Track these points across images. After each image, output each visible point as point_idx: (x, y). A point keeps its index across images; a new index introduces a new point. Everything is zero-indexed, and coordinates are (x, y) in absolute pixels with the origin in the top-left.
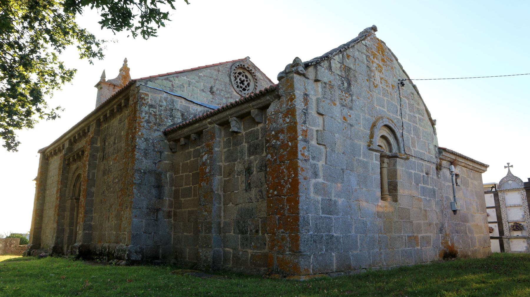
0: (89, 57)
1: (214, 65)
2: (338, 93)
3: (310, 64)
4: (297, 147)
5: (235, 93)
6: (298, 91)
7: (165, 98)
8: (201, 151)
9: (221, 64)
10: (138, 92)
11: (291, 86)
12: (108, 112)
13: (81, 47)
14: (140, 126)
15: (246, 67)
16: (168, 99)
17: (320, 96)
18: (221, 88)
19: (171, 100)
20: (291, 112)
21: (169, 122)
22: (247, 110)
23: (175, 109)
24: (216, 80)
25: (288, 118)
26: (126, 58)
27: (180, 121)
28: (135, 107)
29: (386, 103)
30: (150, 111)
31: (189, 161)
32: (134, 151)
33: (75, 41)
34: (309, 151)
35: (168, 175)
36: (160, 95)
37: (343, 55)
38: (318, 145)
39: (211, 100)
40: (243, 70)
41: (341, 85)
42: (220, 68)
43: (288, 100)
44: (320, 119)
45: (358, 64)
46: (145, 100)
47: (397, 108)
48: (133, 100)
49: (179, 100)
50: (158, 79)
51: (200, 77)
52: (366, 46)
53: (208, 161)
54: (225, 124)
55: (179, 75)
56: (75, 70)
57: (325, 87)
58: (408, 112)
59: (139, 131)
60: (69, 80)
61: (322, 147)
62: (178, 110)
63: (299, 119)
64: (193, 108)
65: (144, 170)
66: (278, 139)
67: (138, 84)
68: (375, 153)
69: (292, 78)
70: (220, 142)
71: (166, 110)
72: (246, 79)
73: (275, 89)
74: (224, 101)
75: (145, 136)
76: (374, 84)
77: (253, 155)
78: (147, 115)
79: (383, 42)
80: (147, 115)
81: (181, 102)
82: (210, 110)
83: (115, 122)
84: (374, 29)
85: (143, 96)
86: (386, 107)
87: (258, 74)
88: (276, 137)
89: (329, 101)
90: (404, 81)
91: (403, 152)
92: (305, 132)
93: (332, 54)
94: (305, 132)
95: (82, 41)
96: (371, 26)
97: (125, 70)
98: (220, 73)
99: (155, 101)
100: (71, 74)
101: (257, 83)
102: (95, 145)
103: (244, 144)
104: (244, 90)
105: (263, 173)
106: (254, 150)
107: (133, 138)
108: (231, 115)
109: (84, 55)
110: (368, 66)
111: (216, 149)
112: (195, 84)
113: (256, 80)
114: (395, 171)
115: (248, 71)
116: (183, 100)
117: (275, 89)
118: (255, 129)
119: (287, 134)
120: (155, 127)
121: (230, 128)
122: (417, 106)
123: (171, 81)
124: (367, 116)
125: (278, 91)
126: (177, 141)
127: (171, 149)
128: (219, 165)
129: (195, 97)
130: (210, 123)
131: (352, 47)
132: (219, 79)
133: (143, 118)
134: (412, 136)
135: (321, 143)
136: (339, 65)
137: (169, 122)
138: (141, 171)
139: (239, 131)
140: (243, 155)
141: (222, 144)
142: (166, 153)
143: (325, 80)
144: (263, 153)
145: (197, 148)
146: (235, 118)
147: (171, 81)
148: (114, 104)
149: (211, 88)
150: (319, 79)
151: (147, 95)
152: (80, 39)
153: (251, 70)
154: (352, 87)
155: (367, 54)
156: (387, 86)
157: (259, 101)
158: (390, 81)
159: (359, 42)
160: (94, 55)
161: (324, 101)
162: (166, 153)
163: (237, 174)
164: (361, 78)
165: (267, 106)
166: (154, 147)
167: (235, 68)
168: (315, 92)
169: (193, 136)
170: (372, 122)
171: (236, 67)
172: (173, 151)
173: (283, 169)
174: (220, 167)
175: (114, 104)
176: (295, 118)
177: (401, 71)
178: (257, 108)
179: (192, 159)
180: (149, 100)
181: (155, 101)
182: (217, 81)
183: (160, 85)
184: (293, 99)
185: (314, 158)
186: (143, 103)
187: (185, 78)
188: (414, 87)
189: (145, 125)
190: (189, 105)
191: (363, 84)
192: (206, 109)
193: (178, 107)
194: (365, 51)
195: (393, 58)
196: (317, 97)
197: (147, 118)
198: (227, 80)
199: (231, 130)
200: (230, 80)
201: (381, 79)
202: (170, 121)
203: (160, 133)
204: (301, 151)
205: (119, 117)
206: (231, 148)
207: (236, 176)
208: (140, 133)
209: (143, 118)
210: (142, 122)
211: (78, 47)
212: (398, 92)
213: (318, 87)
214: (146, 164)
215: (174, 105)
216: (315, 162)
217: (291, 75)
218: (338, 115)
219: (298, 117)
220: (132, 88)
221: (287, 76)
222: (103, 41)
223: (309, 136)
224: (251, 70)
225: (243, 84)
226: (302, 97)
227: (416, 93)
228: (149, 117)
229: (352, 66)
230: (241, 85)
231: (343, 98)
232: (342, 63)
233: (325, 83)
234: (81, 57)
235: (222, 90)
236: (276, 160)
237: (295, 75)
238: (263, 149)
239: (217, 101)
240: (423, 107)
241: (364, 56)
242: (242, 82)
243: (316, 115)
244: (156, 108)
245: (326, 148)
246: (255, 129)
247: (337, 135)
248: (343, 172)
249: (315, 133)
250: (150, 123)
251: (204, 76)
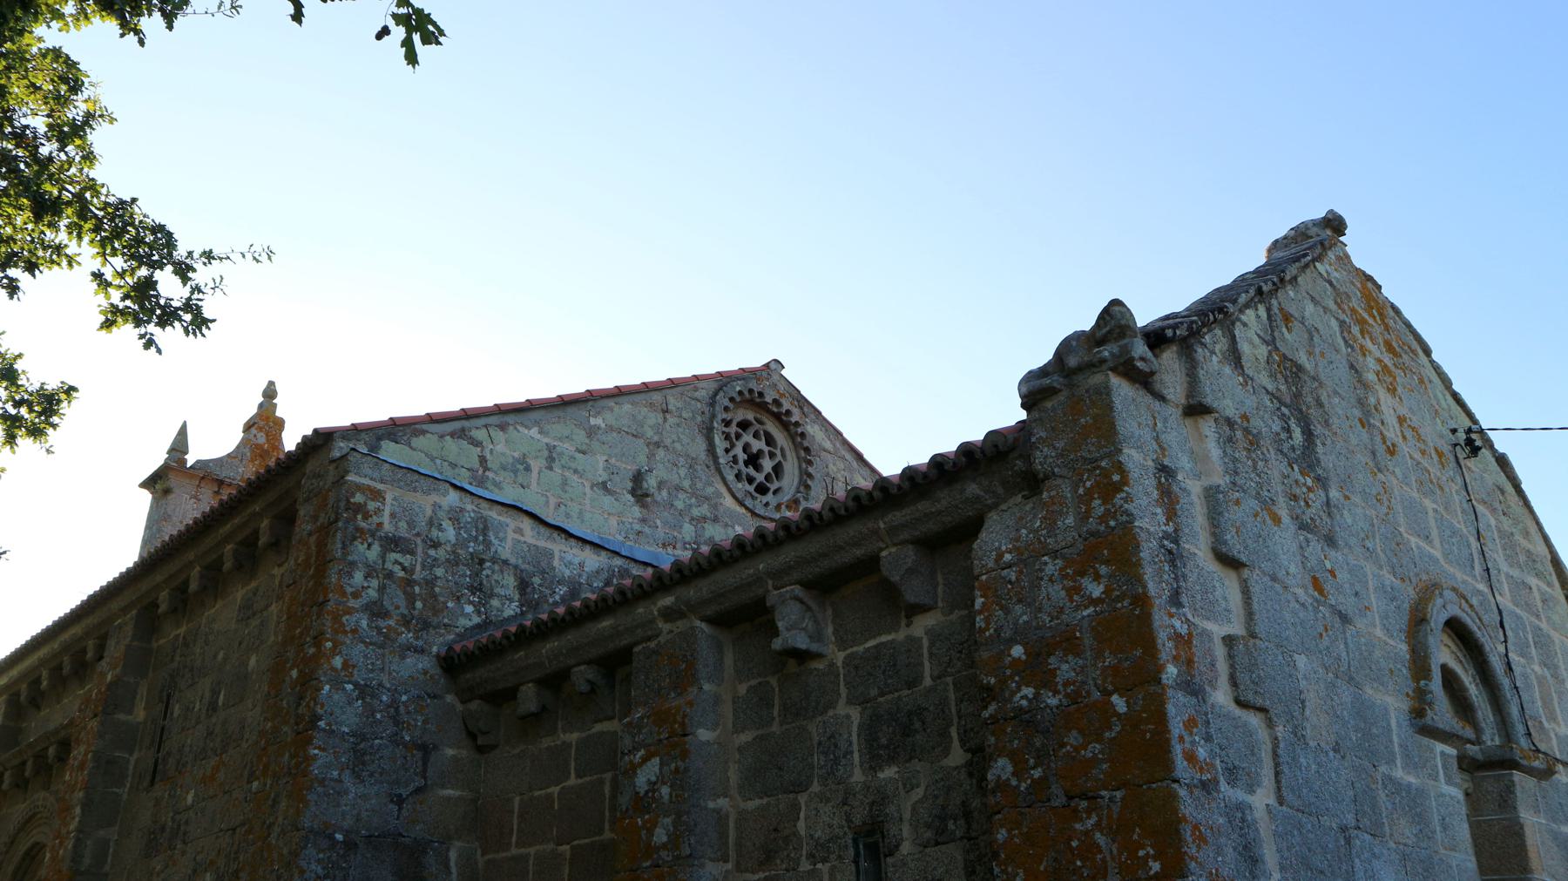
0: (138, 323)
1: (647, 388)
2: (1276, 468)
3: (1169, 333)
4: (1161, 719)
5: (729, 502)
6: (1133, 452)
7: (451, 509)
8: (627, 742)
9: (672, 384)
10: (340, 480)
11: (1106, 429)
12: (196, 571)
13: (108, 274)
14: (340, 629)
15: (768, 399)
16: (467, 517)
17: (1220, 479)
18: (675, 479)
19: (475, 521)
20: (1113, 547)
21: (469, 615)
22: (859, 552)
23: (494, 560)
24: (657, 445)
25: (1097, 578)
26: (271, 383)
27: (511, 610)
28: (322, 545)
29: (1432, 523)
30: (389, 565)
31: (555, 790)
32: (309, 741)
33: (86, 252)
34: (1208, 738)
35: (453, 855)
36: (434, 498)
37: (1269, 310)
38: (1238, 711)
39: (637, 527)
40: (756, 412)
41: (1284, 436)
42: (671, 400)
43: (1089, 494)
44: (1228, 587)
46: (366, 516)
47: (1469, 546)
48: (315, 518)
49: (510, 521)
50: (424, 432)
51: (591, 432)
53: (665, 790)
54: (747, 619)
55: (510, 419)
56: (70, 390)
57: (1230, 440)
58: (1504, 567)
59: (335, 650)
60: (36, 432)
61: (1254, 720)
62: (505, 562)
63: (1156, 586)
64: (569, 557)
65: (347, 833)
66: (1046, 680)
67: (339, 448)
68: (1440, 747)
69: (1105, 392)
70: (717, 700)
71: (454, 562)
72: (766, 449)
73: (1013, 449)
74: (688, 531)
75: (359, 677)
77: (892, 760)
78: (375, 583)
79: (1370, 278)
80: (375, 583)
81: (519, 531)
82: (636, 571)
83: (222, 615)
84: (1335, 224)
85: (359, 498)
86: (1437, 542)
87: (812, 430)
88: (1036, 670)
89: (1253, 503)
90: (1474, 442)
91: (1523, 742)
92: (1183, 641)
93: (1234, 302)
94: (1183, 641)
95: (114, 253)
96: (1320, 214)
97: (265, 422)
98: (671, 420)
99: (411, 524)
100: (49, 404)
101: (810, 463)
102: (122, 717)
103: (842, 709)
104: (762, 490)
105: (955, 852)
106: (894, 736)
107: (308, 682)
108: (779, 576)
109: (124, 313)
110: (1352, 367)
111: (704, 735)
112: (573, 458)
113: (805, 451)
114: (1515, 832)
115: (777, 417)
116: (527, 524)
117: (1013, 449)
118: (900, 635)
119: (1099, 655)
120: (407, 636)
121: (775, 633)
122: (1524, 543)
123: (477, 444)
124: (1389, 579)
125: (1028, 458)
126: (502, 697)
127: (472, 736)
128: (718, 811)
129: (574, 515)
130: (669, 615)
131: (1290, 282)
132: (668, 442)
133: (356, 595)
134: (1536, 668)
135: (1250, 697)
136: (1263, 351)
137: (468, 616)
138: (331, 837)
139: (814, 647)
140: (836, 761)
141: (727, 710)
142: (450, 752)
144: (946, 752)
145: (598, 728)
146: (797, 590)
147: (477, 444)
148: (226, 539)
149: (638, 478)
151: (377, 495)
152: (104, 247)
153: (788, 413)
154: (1320, 449)
155: (1342, 317)
156: (1423, 453)
157: (923, 506)
159: (1307, 266)
160: (168, 317)
161: (1237, 502)
162: (450, 752)
163: (811, 856)
164: (1341, 409)
165: (971, 528)
166: (397, 723)
167: (726, 402)
168: (1200, 458)
169: (583, 676)
170: (1406, 606)
171: (732, 399)
172: (478, 741)
173: (1087, 833)
174: (721, 818)
175: (226, 539)
176: (1140, 580)
178: (912, 543)
179: (573, 781)
180: (386, 519)
181: (411, 524)
182: (661, 453)
183: (433, 459)
184: (1117, 488)
185: (1232, 773)
186: (358, 529)
187: (534, 432)
188: (1502, 461)
189: (364, 623)
190: (549, 545)
191: (1354, 441)
192: (618, 562)
193: (505, 552)
196: (1206, 482)
197: (373, 593)
198: (700, 447)
199: (777, 644)
200: (711, 450)
202: (469, 609)
203: (425, 663)
204: (1181, 738)
205: (240, 594)
206: (775, 728)
207: (805, 866)
208: (338, 662)
209: (356, 595)
210: (349, 611)
211: (97, 276)
212: (1459, 480)
213: (1202, 438)
214: (355, 802)
215: (488, 544)
216: (1238, 795)
217: (1096, 379)
218: (1293, 569)
219: (1148, 573)
220: (311, 466)
221: (1071, 386)
222: (208, 256)
223: (1201, 665)
224: (788, 413)
225: (758, 468)
226: (1154, 482)
227: (1509, 488)
228: (382, 589)
230: (751, 470)
231: (1297, 491)
232: (1271, 342)
233: (1230, 423)
234: (108, 324)
235: (679, 488)
236: (1040, 785)
237: (1115, 380)
238: (944, 734)
239: (661, 533)
240: (1542, 549)
241: (1334, 324)
242: (753, 460)
243: (1212, 566)
244: (412, 553)
245: (1270, 724)
246: (900, 635)
247: (1301, 661)
248: (1348, 841)
249: (1220, 651)
250: (385, 615)
251: (610, 428)
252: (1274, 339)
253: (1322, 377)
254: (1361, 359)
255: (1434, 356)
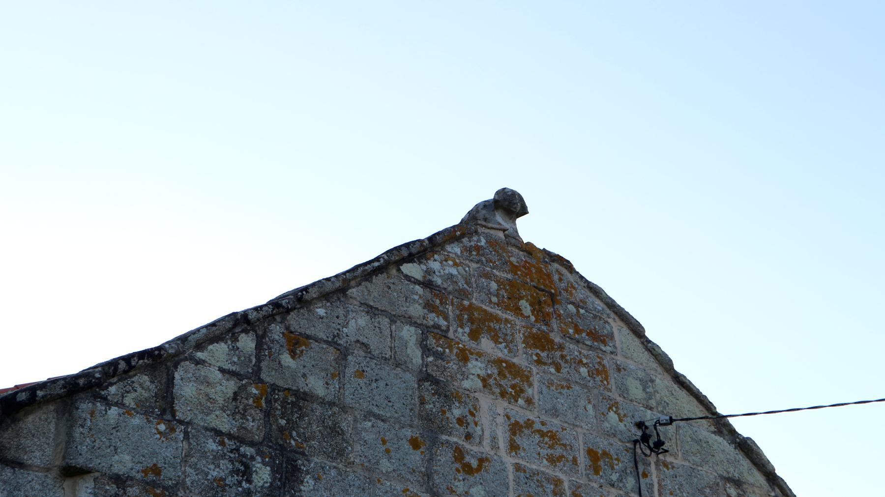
45: (361, 374)
52: (427, 284)
76: (459, 454)
84: (509, 204)
143: (124, 463)
150: (81, 461)
156: (553, 460)
158: (579, 440)
177: (662, 382)
188: (747, 448)
194: (416, 310)
195: (616, 326)
201: (515, 428)
227: (758, 478)
229: (316, 385)
241: (409, 333)
252: (258, 370)
253: (348, 401)
254: (453, 366)
255: (649, 334)
